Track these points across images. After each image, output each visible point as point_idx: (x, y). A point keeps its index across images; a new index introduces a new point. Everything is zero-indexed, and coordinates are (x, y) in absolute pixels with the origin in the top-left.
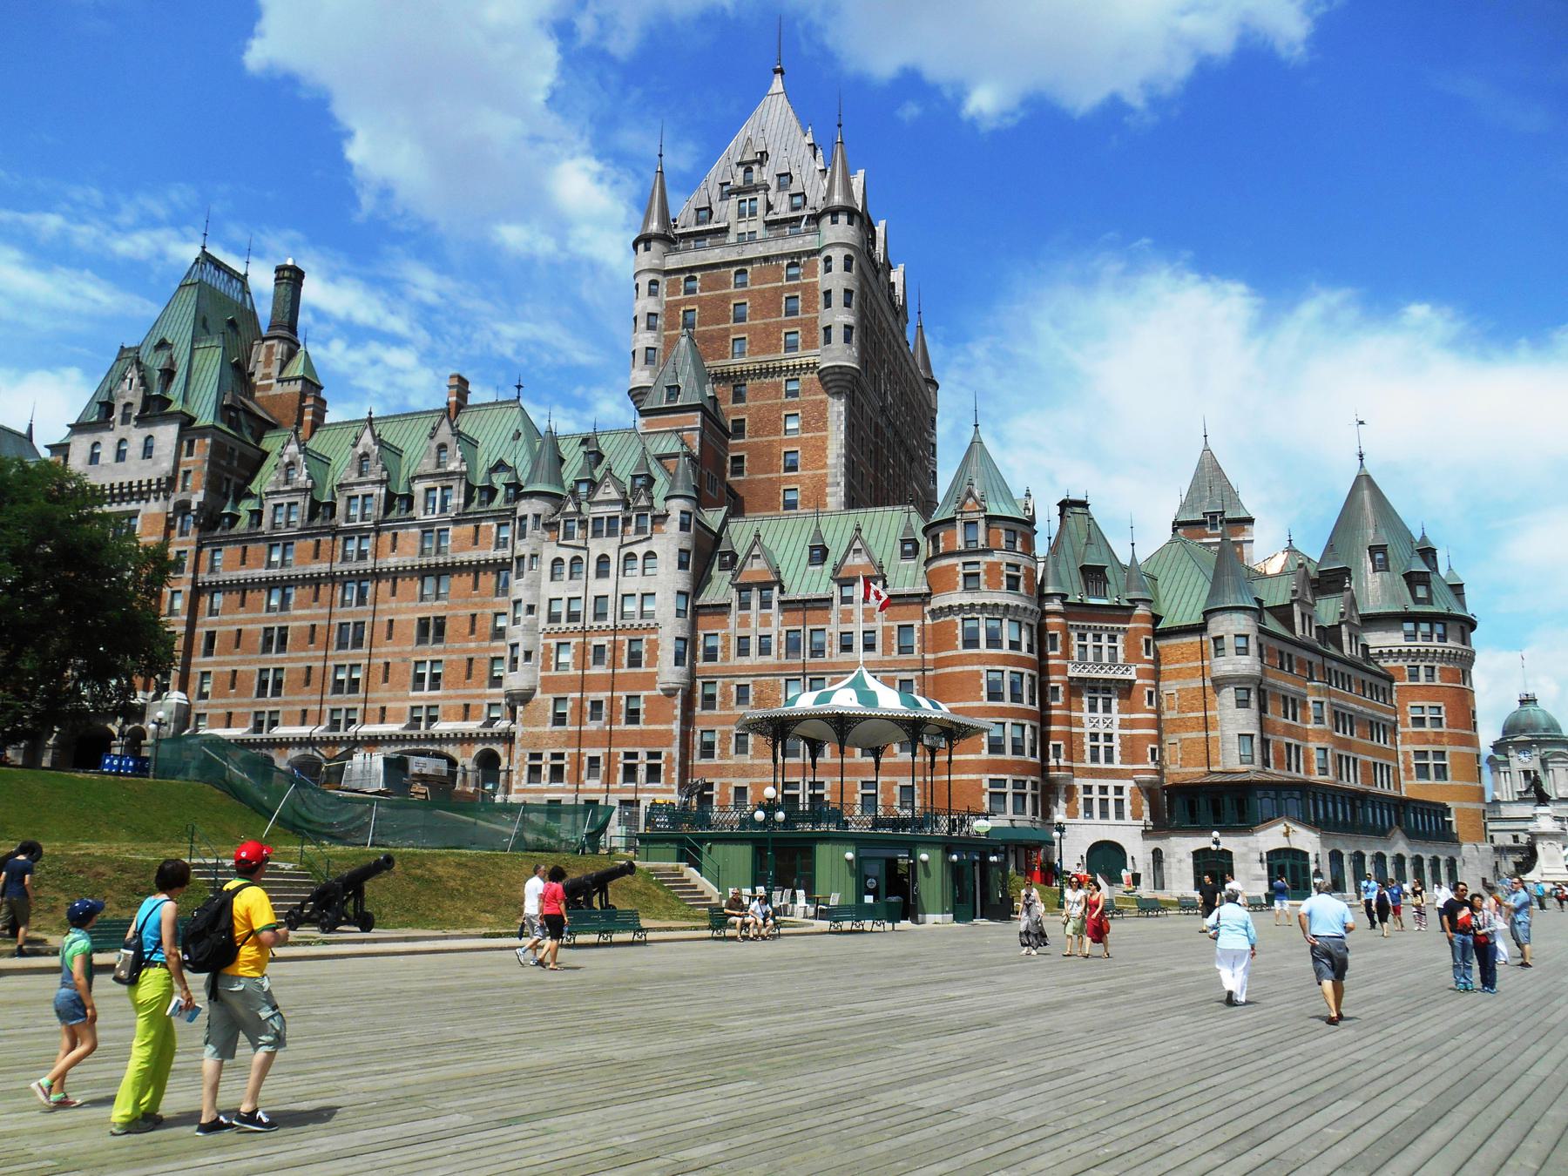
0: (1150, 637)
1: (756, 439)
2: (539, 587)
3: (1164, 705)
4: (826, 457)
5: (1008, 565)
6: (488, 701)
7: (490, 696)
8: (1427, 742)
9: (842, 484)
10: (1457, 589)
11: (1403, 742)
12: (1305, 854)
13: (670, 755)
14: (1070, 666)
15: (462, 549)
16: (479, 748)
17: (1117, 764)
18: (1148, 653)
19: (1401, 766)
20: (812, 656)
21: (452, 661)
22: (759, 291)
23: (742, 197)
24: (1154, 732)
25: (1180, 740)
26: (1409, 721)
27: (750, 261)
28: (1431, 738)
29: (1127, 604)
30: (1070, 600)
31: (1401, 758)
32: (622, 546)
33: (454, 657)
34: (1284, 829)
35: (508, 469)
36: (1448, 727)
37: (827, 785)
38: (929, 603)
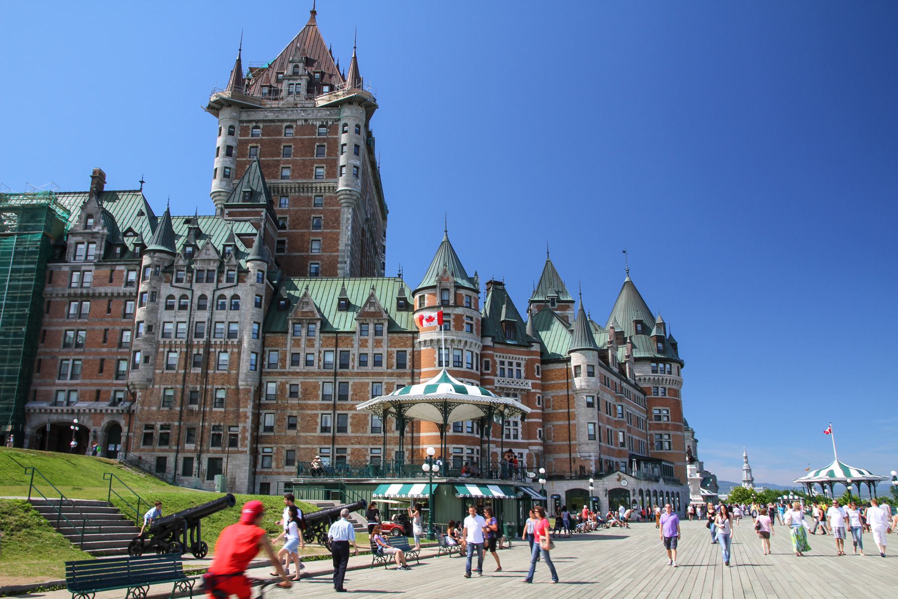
0: (539, 365)
1: (294, 231)
2: (157, 313)
3: (545, 405)
4: (339, 245)
5: (467, 317)
6: (114, 388)
7: (116, 385)
8: (662, 429)
9: (348, 262)
10: (674, 345)
11: (649, 430)
12: (629, 491)
13: (244, 428)
14: (496, 379)
15: (101, 285)
16: (105, 421)
17: (520, 440)
18: (538, 374)
19: (649, 443)
20: (341, 368)
21: (89, 360)
22: (300, 139)
23: (291, 82)
24: (540, 420)
25: (553, 426)
26: (653, 417)
27: (295, 121)
28: (664, 427)
29: (527, 344)
30: (497, 340)
31: (648, 437)
32: (218, 289)
33: (91, 357)
34: (618, 477)
35: (136, 235)
36: (672, 421)
37: (349, 451)
38: (417, 338)
